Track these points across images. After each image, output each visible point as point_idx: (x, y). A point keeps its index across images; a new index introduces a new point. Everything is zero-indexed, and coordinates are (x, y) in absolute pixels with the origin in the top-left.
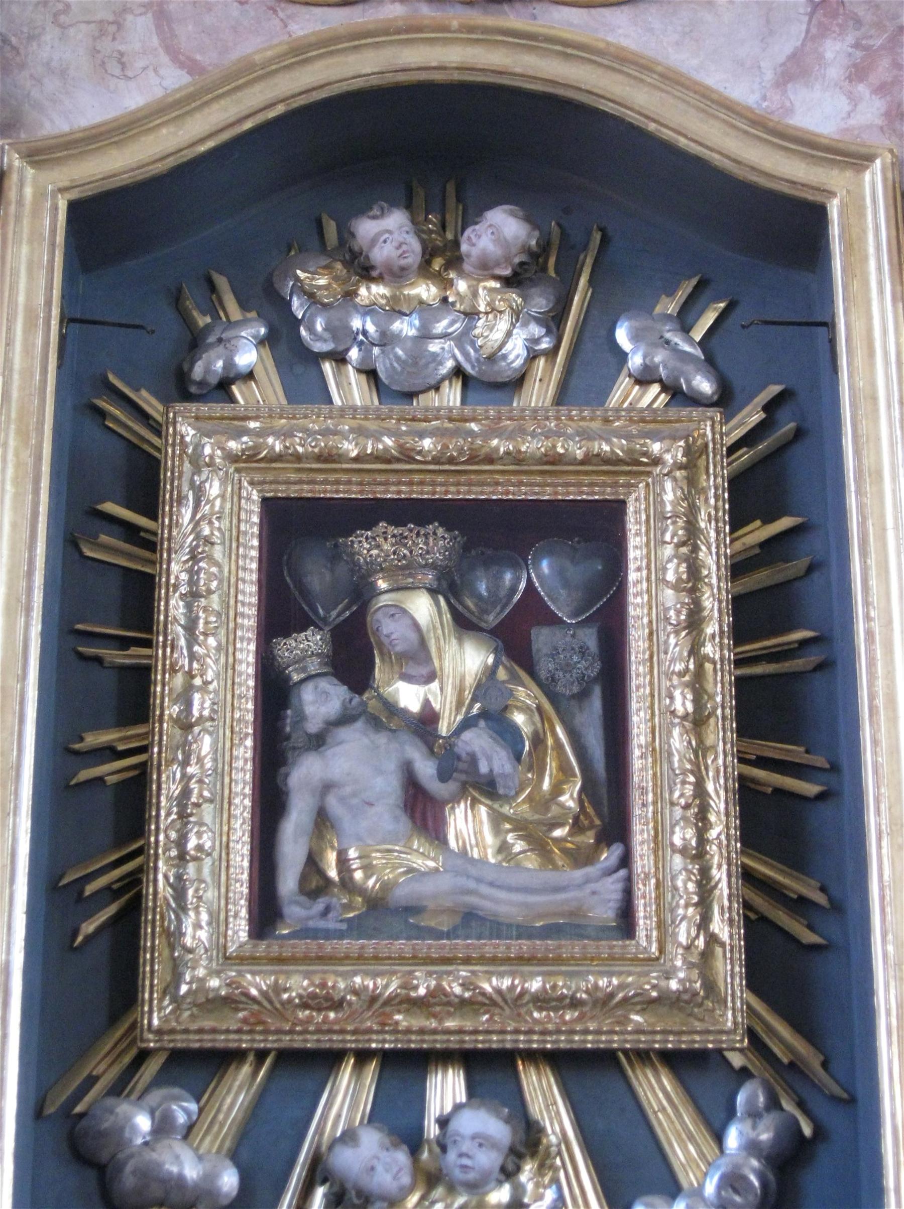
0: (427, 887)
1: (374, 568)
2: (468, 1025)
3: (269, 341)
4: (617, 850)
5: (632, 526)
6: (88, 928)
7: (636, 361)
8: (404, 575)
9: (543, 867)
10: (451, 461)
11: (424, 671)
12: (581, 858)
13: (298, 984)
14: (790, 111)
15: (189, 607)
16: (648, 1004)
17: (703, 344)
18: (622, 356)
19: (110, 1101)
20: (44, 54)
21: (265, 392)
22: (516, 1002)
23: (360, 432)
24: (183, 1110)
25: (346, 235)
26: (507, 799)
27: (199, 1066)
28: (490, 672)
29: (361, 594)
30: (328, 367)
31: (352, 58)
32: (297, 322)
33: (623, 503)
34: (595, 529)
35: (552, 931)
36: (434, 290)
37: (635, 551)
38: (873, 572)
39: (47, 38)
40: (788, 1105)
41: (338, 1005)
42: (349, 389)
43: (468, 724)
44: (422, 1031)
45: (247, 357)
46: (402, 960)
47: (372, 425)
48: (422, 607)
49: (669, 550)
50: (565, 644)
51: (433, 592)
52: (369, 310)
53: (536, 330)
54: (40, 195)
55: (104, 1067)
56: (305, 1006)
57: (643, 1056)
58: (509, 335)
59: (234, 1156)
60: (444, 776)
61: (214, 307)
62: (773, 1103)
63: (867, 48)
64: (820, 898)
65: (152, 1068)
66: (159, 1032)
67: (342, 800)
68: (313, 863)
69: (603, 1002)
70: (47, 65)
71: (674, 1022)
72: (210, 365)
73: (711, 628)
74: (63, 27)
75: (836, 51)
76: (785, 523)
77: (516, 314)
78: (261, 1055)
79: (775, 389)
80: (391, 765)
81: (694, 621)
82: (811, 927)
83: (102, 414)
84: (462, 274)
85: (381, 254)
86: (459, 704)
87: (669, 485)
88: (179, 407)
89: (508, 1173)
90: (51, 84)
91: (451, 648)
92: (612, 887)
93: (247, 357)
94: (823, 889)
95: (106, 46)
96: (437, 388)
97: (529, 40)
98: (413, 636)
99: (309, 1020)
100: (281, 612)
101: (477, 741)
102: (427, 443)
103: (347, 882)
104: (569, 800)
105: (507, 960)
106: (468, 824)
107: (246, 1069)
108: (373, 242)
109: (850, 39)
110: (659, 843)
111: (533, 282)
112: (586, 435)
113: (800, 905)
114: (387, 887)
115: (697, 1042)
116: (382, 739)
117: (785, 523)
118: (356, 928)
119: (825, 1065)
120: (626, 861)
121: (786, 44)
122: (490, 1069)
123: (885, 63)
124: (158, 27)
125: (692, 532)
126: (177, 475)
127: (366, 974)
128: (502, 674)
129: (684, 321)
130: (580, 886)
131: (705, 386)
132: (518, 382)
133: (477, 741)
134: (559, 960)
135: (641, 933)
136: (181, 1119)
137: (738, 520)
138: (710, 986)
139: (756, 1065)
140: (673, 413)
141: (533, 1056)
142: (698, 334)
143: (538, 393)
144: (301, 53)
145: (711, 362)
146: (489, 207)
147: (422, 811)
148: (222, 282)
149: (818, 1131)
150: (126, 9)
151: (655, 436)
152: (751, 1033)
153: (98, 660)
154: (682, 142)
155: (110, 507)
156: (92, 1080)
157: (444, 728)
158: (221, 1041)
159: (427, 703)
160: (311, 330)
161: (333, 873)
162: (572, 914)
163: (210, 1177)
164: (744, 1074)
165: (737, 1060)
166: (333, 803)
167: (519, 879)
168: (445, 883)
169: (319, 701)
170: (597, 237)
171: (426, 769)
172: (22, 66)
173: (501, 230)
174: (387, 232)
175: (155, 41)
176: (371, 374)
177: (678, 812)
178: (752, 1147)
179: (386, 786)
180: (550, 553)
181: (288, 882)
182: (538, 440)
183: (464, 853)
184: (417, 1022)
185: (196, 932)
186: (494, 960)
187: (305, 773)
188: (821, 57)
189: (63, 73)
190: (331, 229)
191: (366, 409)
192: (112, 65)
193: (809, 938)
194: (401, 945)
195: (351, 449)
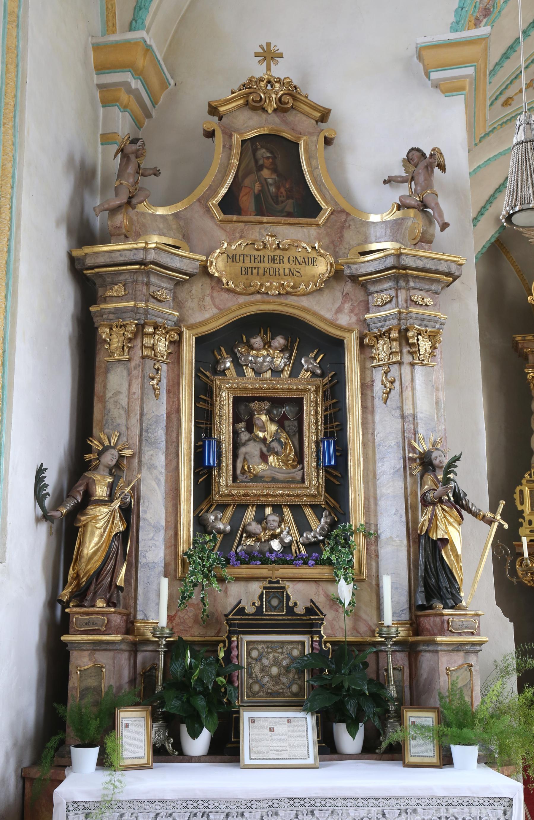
0: (265, 473)
1: (255, 410)
2: (274, 500)
3: (232, 362)
4: (301, 466)
5: (304, 402)
6: (201, 480)
7: (306, 367)
8: (260, 412)
9: (286, 469)
10: (270, 389)
11: (264, 430)
12: (294, 467)
13: (242, 492)
14: (337, 319)
15: (219, 418)
18: (303, 366)
19: (206, 514)
20: (189, 305)
21: (232, 373)
22: (282, 495)
23: (252, 383)
24: (220, 515)
25: (248, 341)
26: (280, 456)
27: (222, 507)
28: (277, 431)
29: (252, 415)
30: (244, 367)
31: (251, 307)
32: (238, 358)
33: (303, 398)
35: (288, 482)
36: (266, 352)
37: (305, 408)
38: (351, 416)
39: (189, 301)
41: (249, 496)
42: (249, 373)
43: (273, 441)
44: (265, 501)
45: (228, 364)
46: (261, 487)
47: (254, 382)
48: (264, 418)
49: (312, 408)
50: (292, 424)
51: (266, 415)
52: (252, 356)
53: (286, 360)
54: (190, 336)
55: (204, 507)
56: (243, 496)
57: (306, 506)
58: (280, 362)
59: (229, 524)
60: (268, 451)
62: (330, 514)
63: (354, 306)
64: (340, 475)
65: (214, 507)
66: (216, 501)
67: (249, 456)
68: (243, 467)
69: (298, 496)
70: (189, 307)
71: (312, 499)
73: (320, 423)
74: (192, 299)
76: (335, 401)
78: (234, 505)
80: (258, 449)
81: (317, 422)
82: (338, 481)
83: (199, 377)
84: (271, 349)
85: (256, 346)
86: (271, 437)
87: (312, 395)
88: (216, 377)
92: (300, 473)
94: (340, 474)
95: (201, 303)
96: (266, 372)
97: (286, 305)
98: (262, 424)
99: (244, 499)
100: (237, 419)
101: (275, 445)
102: (265, 386)
103: (250, 471)
104: (292, 455)
105: (281, 487)
106: (272, 460)
107: (231, 507)
108: (254, 343)
109: (350, 304)
110: (309, 465)
111: (286, 351)
112: (296, 385)
113: (336, 477)
114: (258, 472)
115: (316, 503)
116: (256, 444)
117: (335, 401)
118: (252, 481)
119: (340, 507)
120: (303, 468)
121: (337, 305)
122: (277, 508)
123: (357, 309)
124: (212, 299)
125: (317, 404)
126: (216, 390)
127: (254, 490)
128: (279, 431)
129: (315, 359)
130: (294, 472)
131: (319, 371)
132: (282, 371)
133: (275, 445)
134: (290, 488)
135: (306, 482)
136: (219, 517)
138: (319, 492)
139: (327, 507)
140: (313, 379)
141: (285, 505)
142: (318, 361)
143: (286, 374)
144: (240, 307)
145: (320, 368)
146: (277, 336)
147: (264, 458)
148: (222, 349)
150: (205, 295)
151: (309, 384)
152: (326, 501)
153: (200, 427)
154: (316, 327)
155: (202, 396)
156: (202, 509)
157: (268, 442)
159: (264, 436)
160: (241, 360)
161: (247, 469)
162: (293, 478)
163: (225, 528)
164: (325, 509)
165: (323, 506)
166: (247, 456)
167: (282, 471)
168: (269, 472)
169: (244, 436)
170: (298, 340)
171: (265, 450)
172: (184, 307)
173: (280, 341)
174: (257, 341)
175: (211, 303)
176: (253, 369)
177: (313, 460)
178: (326, 523)
179: (257, 453)
180: (288, 406)
181: (239, 472)
182: (286, 384)
183: (272, 465)
184: (264, 499)
185: (222, 482)
186: (278, 487)
187: (243, 450)
188: (344, 308)
189: (193, 309)
190: (244, 337)
192: (202, 308)
193: (337, 483)
194: (261, 485)
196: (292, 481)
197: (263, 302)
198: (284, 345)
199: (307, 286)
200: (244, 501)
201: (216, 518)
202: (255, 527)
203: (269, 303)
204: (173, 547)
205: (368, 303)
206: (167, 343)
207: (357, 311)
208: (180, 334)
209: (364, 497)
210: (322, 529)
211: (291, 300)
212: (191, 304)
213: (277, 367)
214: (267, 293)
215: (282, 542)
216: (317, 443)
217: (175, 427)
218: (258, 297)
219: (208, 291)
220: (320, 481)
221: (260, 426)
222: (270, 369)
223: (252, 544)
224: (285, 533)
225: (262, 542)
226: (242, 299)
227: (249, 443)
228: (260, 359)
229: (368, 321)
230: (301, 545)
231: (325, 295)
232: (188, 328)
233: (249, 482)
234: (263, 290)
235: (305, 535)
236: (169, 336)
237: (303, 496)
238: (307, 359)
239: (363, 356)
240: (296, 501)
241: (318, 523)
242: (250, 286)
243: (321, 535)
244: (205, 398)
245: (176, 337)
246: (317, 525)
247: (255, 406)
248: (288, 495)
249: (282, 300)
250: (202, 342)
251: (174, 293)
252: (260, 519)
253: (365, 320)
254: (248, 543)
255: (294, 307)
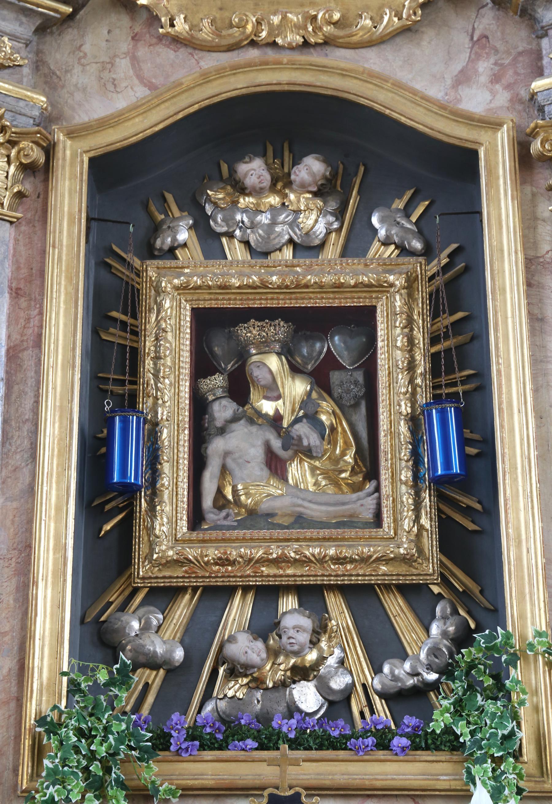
0: (277, 504)
2: (299, 572)
3: (194, 227)
4: (374, 483)
5: (379, 318)
6: (108, 527)
7: (382, 233)
8: (264, 347)
10: (287, 287)
11: (275, 394)
12: (356, 488)
13: (213, 553)
14: (459, 101)
15: (155, 364)
16: (388, 561)
17: (417, 223)
18: (375, 231)
19: (119, 614)
20: (74, 80)
21: (192, 255)
22: (321, 560)
23: (241, 275)
24: (156, 618)
25: (232, 171)
27: (163, 596)
28: (309, 394)
29: (243, 356)
30: (224, 240)
31: (232, 79)
32: (208, 218)
33: (374, 308)
34: (361, 321)
35: (339, 525)
36: (277, 199)
37: (381, 332)
38: (501, 340)
39: (75, 71)
40: (462, 612)
41: (232, 563)
42: (236, 251)
43: (297, 421)
44: (275, 576)
45: (183, 236)
46: (264, 540)
48: (274, 362)
49: (398, 331)
51: (279, 354)
52: (245, 211)
53: (331, 219)
54: (74, 155)
55: (115, 597)
56: (216, 564)
57: (387, 587)
58: (316, 221)
59: (182, 642)
60: (285, 448)
61: (165, 211)
62: (455, 612)
63: (502, 65)
64: (478, 507)
66: (143, 578)
67: (234, 460)
68: (220, 492)
69: (364, 560)
70: (76, 85)
71: (403, 569)
72: (164, 241)
74: (83, 65)
75: (484, 67)
76: (460, 315)
77: (320, 210)
78: (195, 589)
79: (454, 246)
80: (259, 443)
81: (411, 367)
82: (473, 522)
83: (110, 266)
84: (292, 191)
85: (251, 181)
86: (293, 411)
87: (398, 297)
88: (148, 262)
89: (314, 643)
90: (78, 96)
91: (288, 382)
92: (370, 502)
93: (183, 236)
94: (479, 502)
95: (106, 75)
96: (280, 250)
97: (323, 69)
98: (269, 376)
99: (218, 571)
100: (202, 366)
101: (303, 430)
102: (274, 278)
103: (237, 502)
104: (349, 458)
105: (318, 540)
106: (298, 471)
107: (187, 597)
108: (246, 175)
109: (492, 60)
111: (329, 194)
112: (356, 274)
113: (468, 511)
115: (416, 580)
116: (254, 429)
117: (460, 315)
118: (241, 525)
119: (481, 592)
120: (378, 489)
121: (457, 66)
122: (311, 595)
123: (511, 72)
124: (133, 65)
127: (246, 547)
128: (314, 395)
129: (407, 212)
130: (355, 502)
131: (417, 245)
132: (322, 245)
133: (303, 430)
134: (343, 539)
135: (385, 525)
136: (155, 622)
137: (435, 314)
138: (420, 551)
140: (401, 260)
141: (331, 588)
142: (414, 219)
143: (331, 252)
144: (206, 78)
145: (421, 233)
146: (306, 155)
147: (275, 465)
148: (169, 197)
149: (477, 625)
150: (115, 56)
151: (390, 272)
152: (442, 575)
154: (403, 119)
155: (114, 314)
156: (110, 604)
157: (285, 424)
158: (174, 583)
159: (277, 411)
160: (216, 222)
161: (230, 497)
162: (351, 516)
163: (171, 651)
165: (436, 590)
166: (230, 463)
167: (324, 499)
168: (287, 501)
169: (223, 410)
170: (362, 169)
171: (276, 444)
172: (63, 87)
173: (311, 168)
174: (254, 170)
175: (131, 72)
176: (247, 243)
177: (404, 463)
178: (444, 634)
179: (257, 453)
180: (338, 333)
181: (208, 502)
182: (332, 275)
183: (296, 486)
184: (273, 571)
186: (311, 539)
187: (216, 447)
188: (476, 71)
189: (84, 90)
190: (225, 168)
191: (244, 262)
193: (472, 527)
194: (265, 533)
195: (235, 282)
196: (349, 522)
197: (263, 64)
198: (324, 177)
199: (376, 21)
200: (219, 576)
201: (146, 628)
202: (247, 648)
203: (278, 65)
204: (13, 705)
205: (540, 57)
206: (12, 169)
207: (509, 77)
208: (49, 150)
209: (544, 555)
210: (434, 651)
211: (339, 57)
212: (80, 77)
213: (307, 234)
214: (274, 44)
215: (323, 688)
216: (413, 421)
217: (31, 382)
218: (253, 54)
219: (125, 46)
220: (425, 521)
221: (263, 383)
222: (291, 241)
223: (240, 695)
224: (332, 661)
225: (267, 689)
226: (210, 61)
227: (235, 426)
228: (264, 219)
229: (540, 98)
230: (377, 698)
231: (424, 43)
232: (71, 134)
233: (234, 528)
234: (264, 34)
235: (386, 669)
236: (19, 152)
237: (378, 560)
238: (386, 212)
239: (528, 189)
240: (360, 575)
241: (422, 634)
242: (231, 26)
243: (430, 668)
244: (123, 317)
245: (37, 155)
246: (422, 643)
247: (250, 331)
248: (338, 560)
249: (314, 57)
250: (109, 172)
251: (38, 52)
252: (265, 627)
253: (533, 96)
254: (230, 693)
255: (344, 73)
